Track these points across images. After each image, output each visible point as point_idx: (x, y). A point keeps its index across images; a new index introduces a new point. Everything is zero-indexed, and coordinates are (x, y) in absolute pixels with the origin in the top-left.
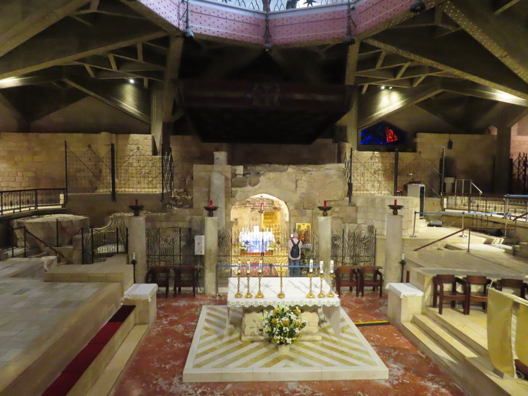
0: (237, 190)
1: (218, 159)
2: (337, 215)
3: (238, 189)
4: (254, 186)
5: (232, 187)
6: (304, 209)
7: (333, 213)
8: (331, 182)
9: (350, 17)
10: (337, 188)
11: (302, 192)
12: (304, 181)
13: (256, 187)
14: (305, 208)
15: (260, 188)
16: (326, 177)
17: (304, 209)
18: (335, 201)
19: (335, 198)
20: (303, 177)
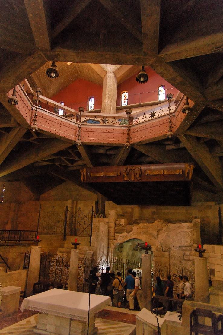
0: (118, 235)
1: (110, 214)
2: (188, 258)
3: (120, 235)
4: (129, 233)
5: (115, 233)
6: (163, 251)
7: (184, 256)
9: (170, 122)
13: (131, 233)
14: (163, 250)
16: (178, 228)
17: (163, 251)
18: (186, 246)
19: (186, 244)
20: (163, 228)
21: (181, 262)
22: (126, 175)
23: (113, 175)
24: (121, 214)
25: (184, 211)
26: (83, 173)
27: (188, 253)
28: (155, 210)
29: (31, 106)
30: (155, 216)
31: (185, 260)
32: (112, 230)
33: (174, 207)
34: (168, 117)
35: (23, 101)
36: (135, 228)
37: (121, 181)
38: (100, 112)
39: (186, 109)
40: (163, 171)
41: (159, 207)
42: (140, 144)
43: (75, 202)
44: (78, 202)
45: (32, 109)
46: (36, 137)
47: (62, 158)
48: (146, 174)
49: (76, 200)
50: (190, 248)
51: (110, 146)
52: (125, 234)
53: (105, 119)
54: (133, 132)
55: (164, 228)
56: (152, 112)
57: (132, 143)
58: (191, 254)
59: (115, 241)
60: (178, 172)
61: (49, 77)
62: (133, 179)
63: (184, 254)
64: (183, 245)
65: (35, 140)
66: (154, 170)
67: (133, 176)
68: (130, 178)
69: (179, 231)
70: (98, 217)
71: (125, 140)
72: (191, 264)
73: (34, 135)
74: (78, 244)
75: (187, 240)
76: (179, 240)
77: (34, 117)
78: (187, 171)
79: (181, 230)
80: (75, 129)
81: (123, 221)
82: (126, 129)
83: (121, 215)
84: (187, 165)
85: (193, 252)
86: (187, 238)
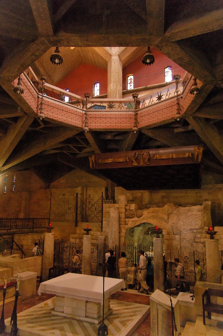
1: (120, 200)
3: (131, 220)
7: (196, 239)
8: (192, 215)
9: (178, 104)
10: (197, 220)
11: (173, 222)
12: (175, 214)
13: (141, 218)
14: (174, 234)
15: (144, 219)
16: (189, 211)
17: (174, 234)
18: (197, 229)
19: (196, 227)
20: (174, 212)
21: (192, 245)
22: (135, 160)
23: (122, 161)
24: (131, 199)
25: (195, 194)
26: (92, 160)
27: (199, 236)
28: (165, 194)
29: (37, 95)
30: (165, 200)
31: (196, 242)
32: (123, 216)
33: (184, 191)
34: (175, 99)
35: (29, 89)
36: (145, 213)
37: (129, 166)
38: (106, 97)
39: (194, 91)
40: (172, 155)
41: (168, 191)
42: (148, 128)
43: (85, 188)
44: (88, 189)
45: (38, 97)
46: (43, 126)
47: (70, 145)
48: (155, 159)
49: (86, 187)
50: (200, 230)
51: (117, 132)
52: (136, 219)
53: (111, 104)
54: (140, 116)
55: (175, 212)
56: (159, 95)
57: (139, 127)
58: (201, 236)
59: (126, 226)
60: (187, 155)
61: (54, 64)
62: (142, 164)
63: (195, 237)
64: (194, 228)
65: (42, 129)
66: (162, 154)
67: (142, 161)
68: (138, 163)
69: (190, 214)
70: (108, 203)
71: (133, 125)
72: (202, 246)
73: (41, 123)
74: (90, 230)
75: (198, 222)
76: (190, 223)
77: (40, 105)
78: (196, 154)
79: (192, 213)
80: (81, 116)
81: (133, 206)
82: (134, 113)
83: (131, 200)
84: (196, 148)
85: (204, 235)
86: (198, 220)
